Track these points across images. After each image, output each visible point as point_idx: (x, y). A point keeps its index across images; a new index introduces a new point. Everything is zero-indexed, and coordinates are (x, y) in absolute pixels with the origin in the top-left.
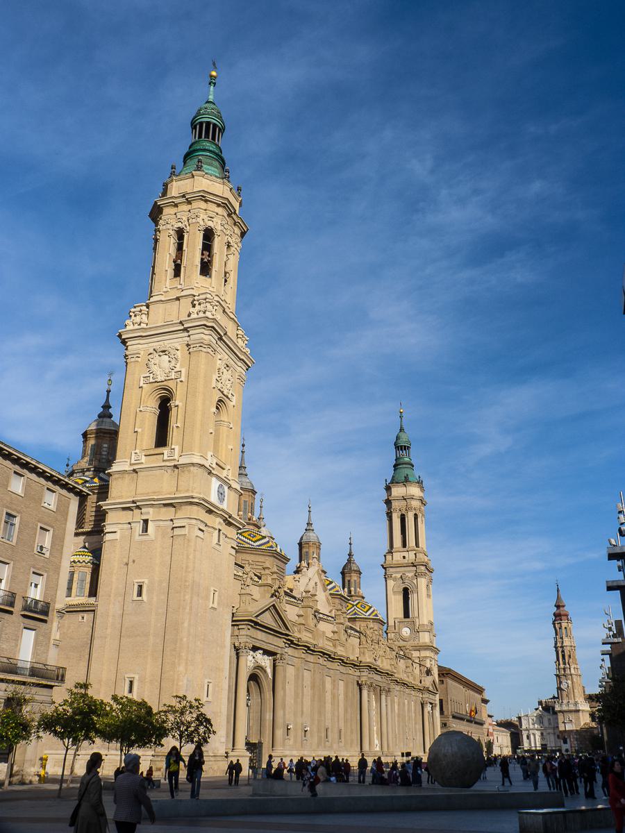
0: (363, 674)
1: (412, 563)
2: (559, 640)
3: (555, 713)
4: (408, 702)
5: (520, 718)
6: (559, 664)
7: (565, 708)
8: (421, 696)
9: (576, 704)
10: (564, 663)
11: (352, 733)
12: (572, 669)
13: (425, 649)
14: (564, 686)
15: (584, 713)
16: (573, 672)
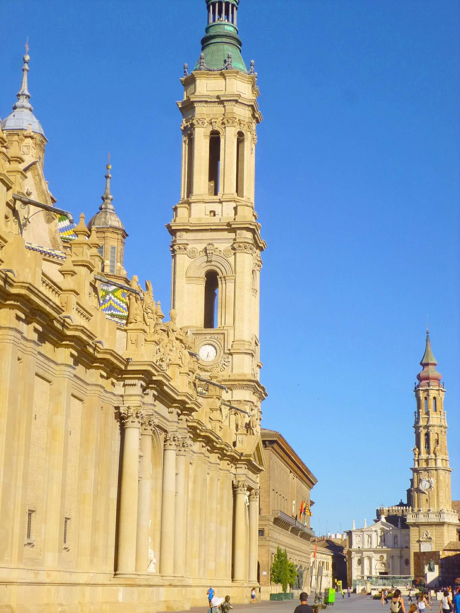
0: (130, 390)
1: (229, 224)
2: (423, 415)
3: (405, 526)
4: (212, 479)
5: (350, 533)
6: (419, 454)
7: (422, 519)
8: (233, 470)
9: (440, 513)
10: (428, 453)
11: (95, 528)
12: (439, 462)
13: (242, 387)
14: (424, 486)
15: (451, 528)
16: (439, 464)
